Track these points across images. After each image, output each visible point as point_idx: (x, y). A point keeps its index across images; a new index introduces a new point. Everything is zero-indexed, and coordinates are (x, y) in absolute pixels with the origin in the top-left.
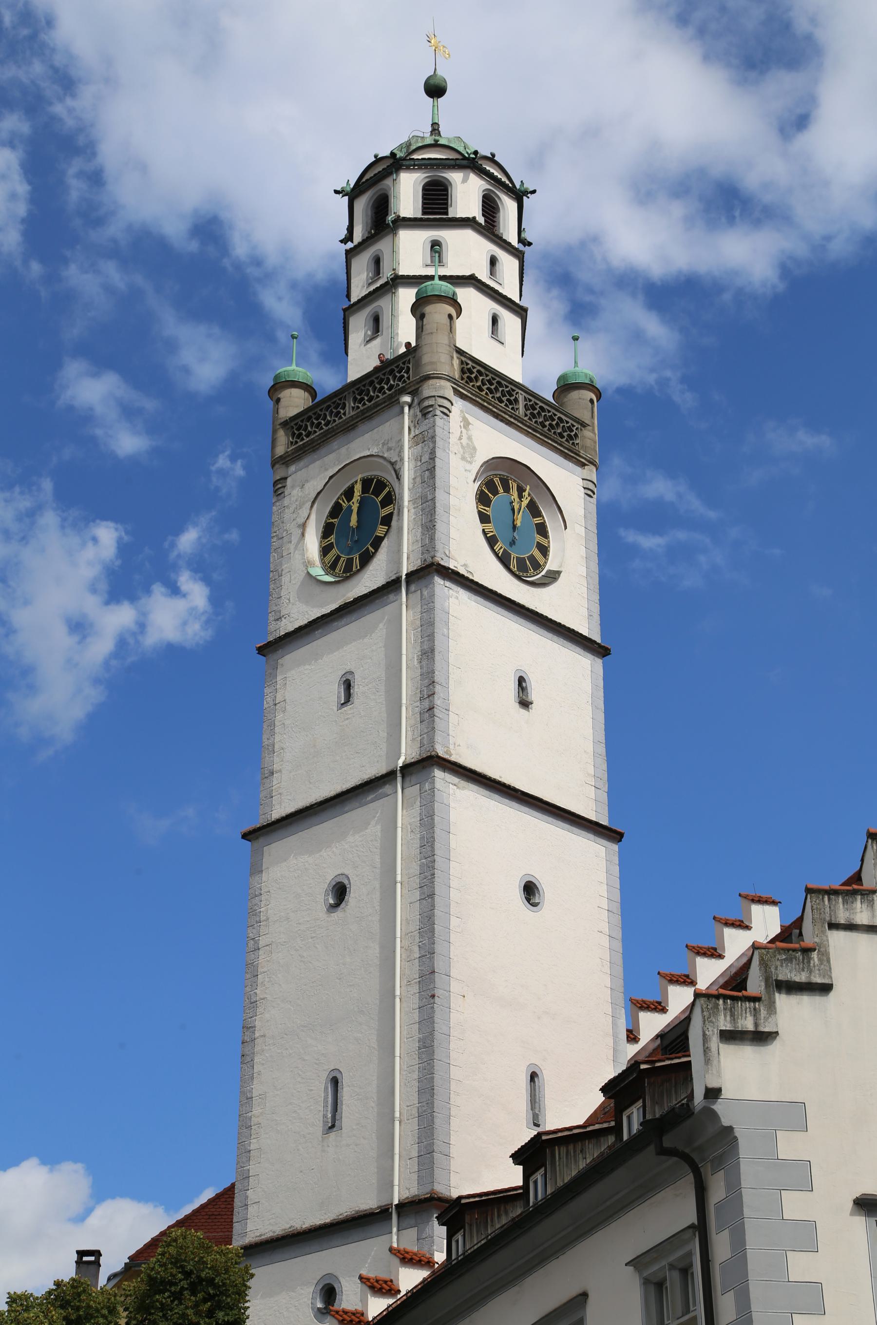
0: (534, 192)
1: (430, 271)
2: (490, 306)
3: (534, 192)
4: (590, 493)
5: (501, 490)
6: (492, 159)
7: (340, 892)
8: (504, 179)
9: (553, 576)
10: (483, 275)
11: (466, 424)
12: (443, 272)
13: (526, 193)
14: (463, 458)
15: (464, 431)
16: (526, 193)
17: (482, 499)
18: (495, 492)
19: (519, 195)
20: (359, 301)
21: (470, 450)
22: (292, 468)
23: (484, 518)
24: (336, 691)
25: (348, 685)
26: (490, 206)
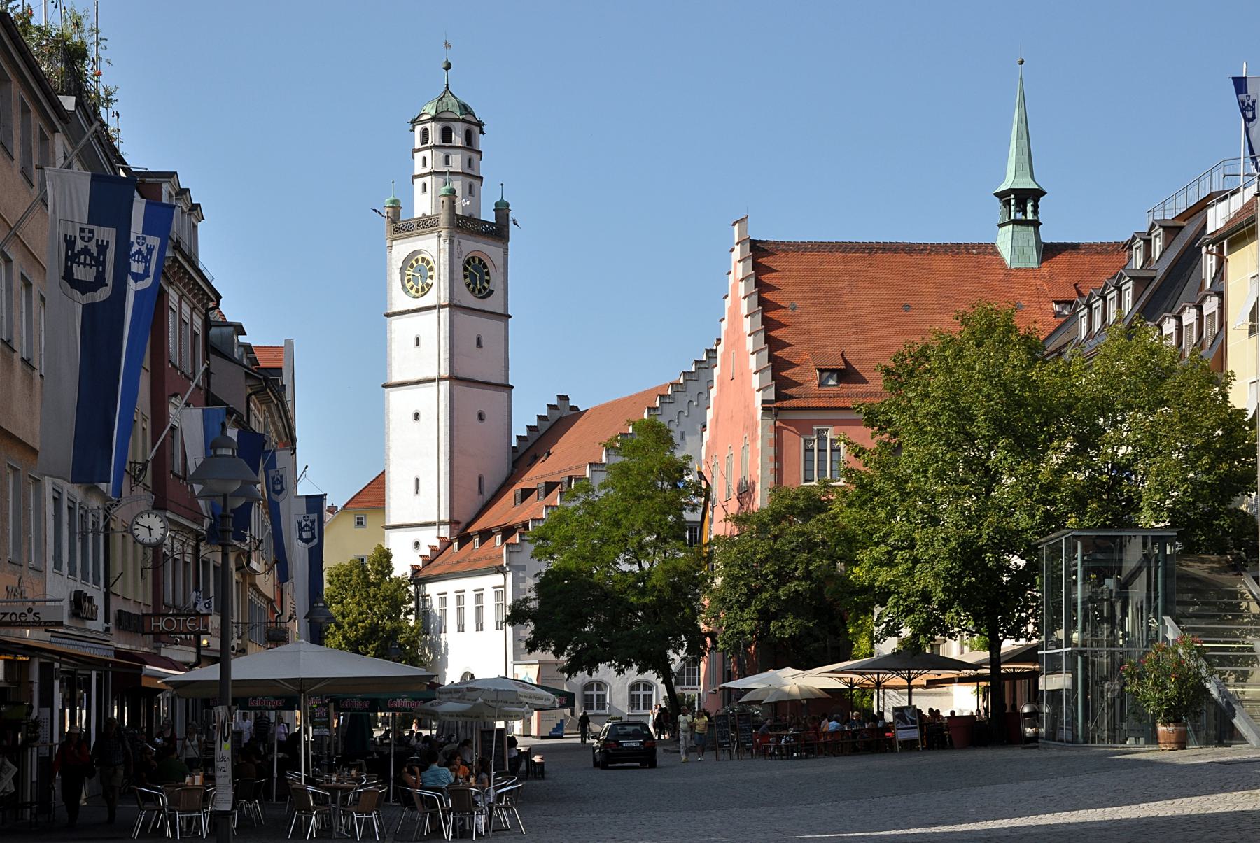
1: (445, 170)
7: (417, 416)
9: (491, 292)
17: (465, 269)
19: (480, 125)
23: (466, 277)
24: (414, 342)
25: (418, 339)
26: (469, 137)
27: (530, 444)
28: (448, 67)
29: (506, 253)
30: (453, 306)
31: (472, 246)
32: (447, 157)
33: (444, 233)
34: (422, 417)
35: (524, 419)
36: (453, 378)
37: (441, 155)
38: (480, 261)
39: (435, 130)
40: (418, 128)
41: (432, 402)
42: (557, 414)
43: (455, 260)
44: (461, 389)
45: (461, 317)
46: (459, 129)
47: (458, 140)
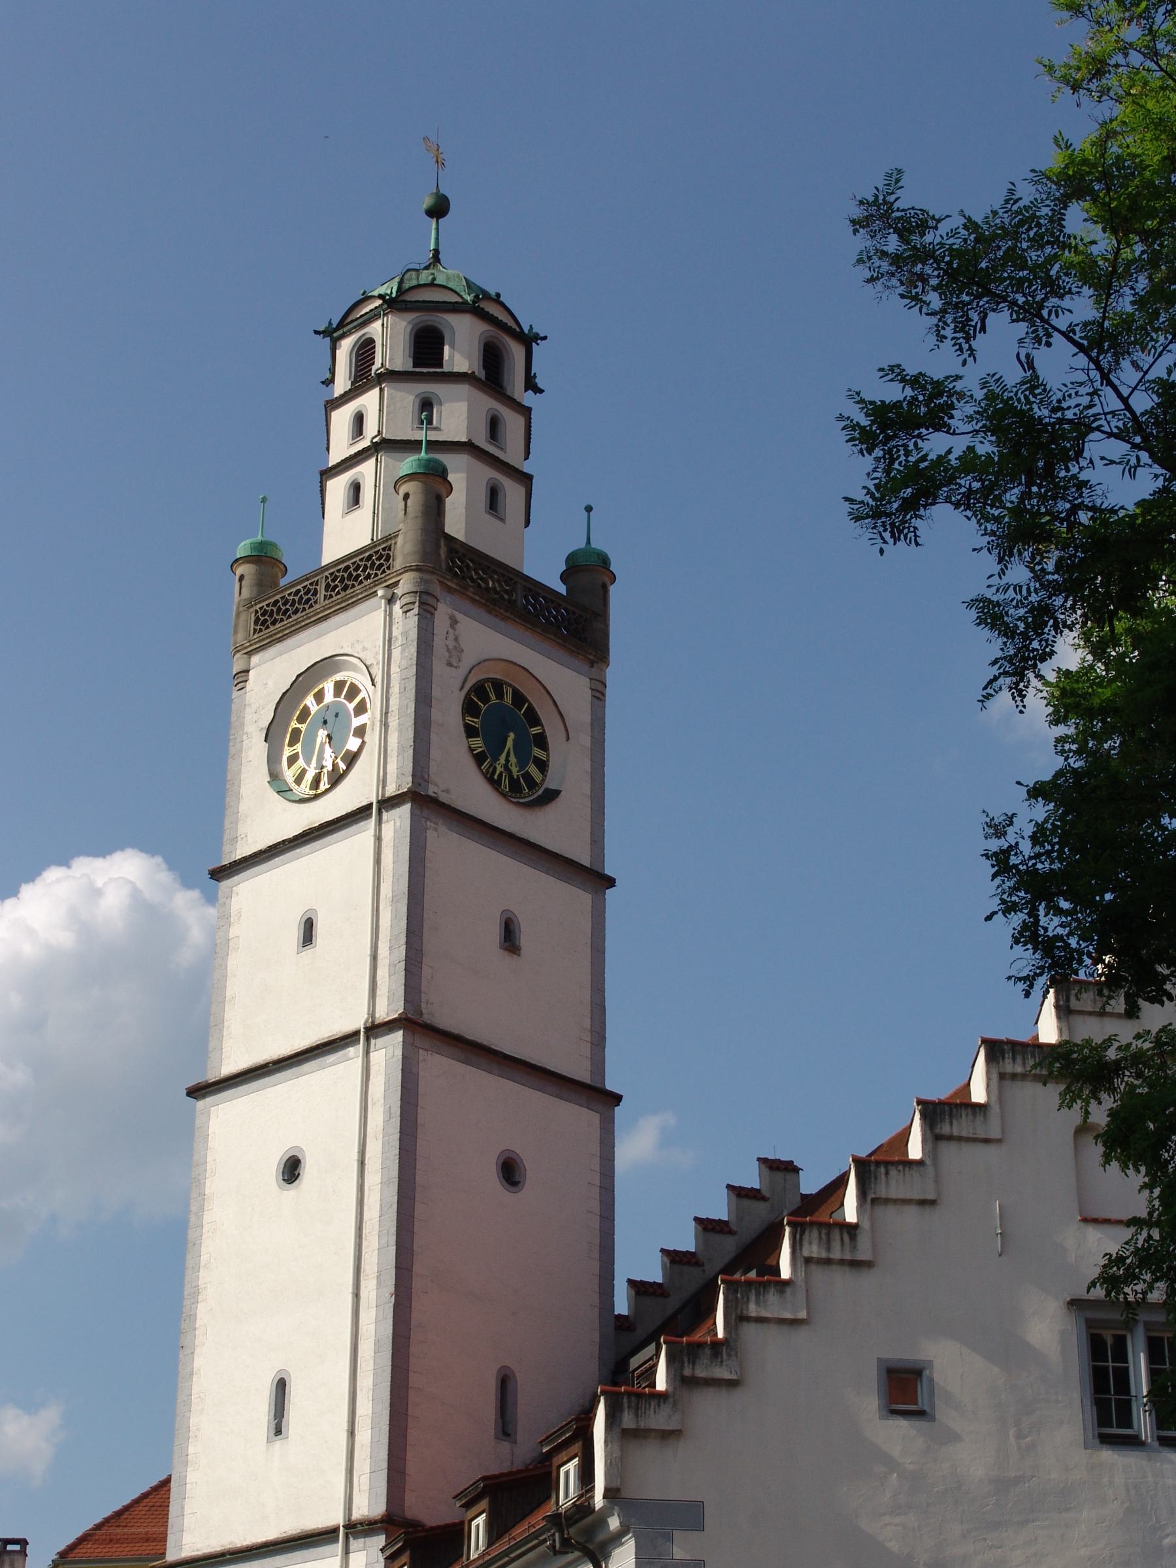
0: (545, 338)
1: (420, 435)
2: (488, 473)
3: (545, 338)
4: (598, 694)
5: (493, 697)
6: (497, 300)
7: (292, 1169)
8: (511, 323)
9: (551, 796)
10: (482, 442)
11: (454, 622)
12: (433, 436)
13: (536, 338)
14: (450, 664)
15: (451, 631)
16: (536, 338)
17: (469, 708)
18: (485, 699)
19: (528, 340)
20: (339, 465)
21: (457, 650)
22: (255, 659)
23: (470, 732)
24: (295, 934)
26: (492, 357)
27: (672, 1304)
28: (439, 209)
29: (599, 694)
30: (423, 800)
31: (487, 642)
32: (426, 405)
33: (406, 584)
34: (308, 1171)
35: (656, 1222)
36: (415, 1025)
37: (406, 398)
38: (519, 699)
39: (390, 338)
40: (346, 346)
41: (342, 1115)
42: (760, 1213)
43: (439, 667)
44: (438, 1066)
45: (446, 842)
46: (467, 344)
47: (459, 356)
